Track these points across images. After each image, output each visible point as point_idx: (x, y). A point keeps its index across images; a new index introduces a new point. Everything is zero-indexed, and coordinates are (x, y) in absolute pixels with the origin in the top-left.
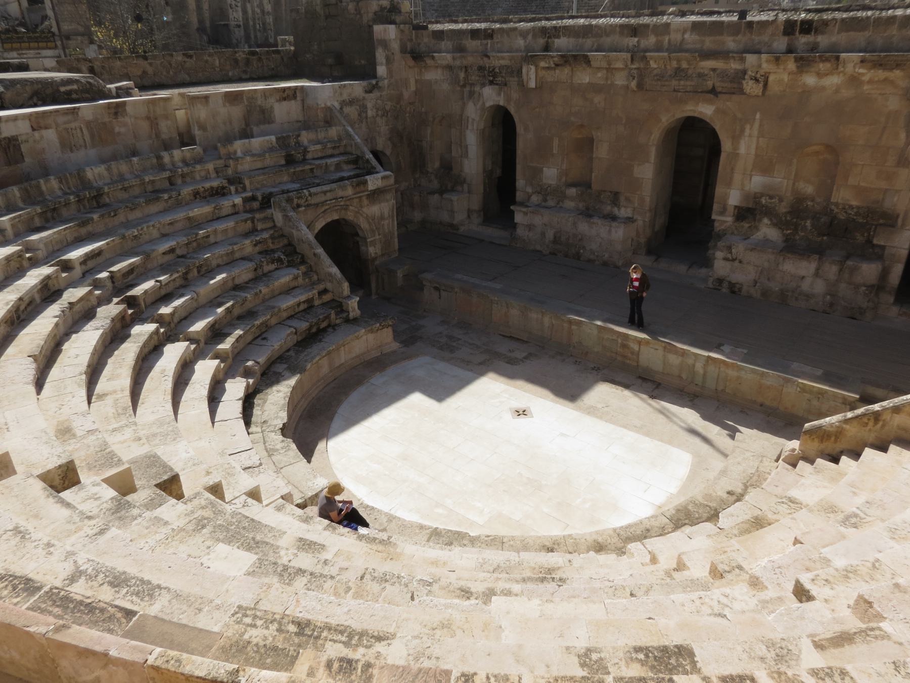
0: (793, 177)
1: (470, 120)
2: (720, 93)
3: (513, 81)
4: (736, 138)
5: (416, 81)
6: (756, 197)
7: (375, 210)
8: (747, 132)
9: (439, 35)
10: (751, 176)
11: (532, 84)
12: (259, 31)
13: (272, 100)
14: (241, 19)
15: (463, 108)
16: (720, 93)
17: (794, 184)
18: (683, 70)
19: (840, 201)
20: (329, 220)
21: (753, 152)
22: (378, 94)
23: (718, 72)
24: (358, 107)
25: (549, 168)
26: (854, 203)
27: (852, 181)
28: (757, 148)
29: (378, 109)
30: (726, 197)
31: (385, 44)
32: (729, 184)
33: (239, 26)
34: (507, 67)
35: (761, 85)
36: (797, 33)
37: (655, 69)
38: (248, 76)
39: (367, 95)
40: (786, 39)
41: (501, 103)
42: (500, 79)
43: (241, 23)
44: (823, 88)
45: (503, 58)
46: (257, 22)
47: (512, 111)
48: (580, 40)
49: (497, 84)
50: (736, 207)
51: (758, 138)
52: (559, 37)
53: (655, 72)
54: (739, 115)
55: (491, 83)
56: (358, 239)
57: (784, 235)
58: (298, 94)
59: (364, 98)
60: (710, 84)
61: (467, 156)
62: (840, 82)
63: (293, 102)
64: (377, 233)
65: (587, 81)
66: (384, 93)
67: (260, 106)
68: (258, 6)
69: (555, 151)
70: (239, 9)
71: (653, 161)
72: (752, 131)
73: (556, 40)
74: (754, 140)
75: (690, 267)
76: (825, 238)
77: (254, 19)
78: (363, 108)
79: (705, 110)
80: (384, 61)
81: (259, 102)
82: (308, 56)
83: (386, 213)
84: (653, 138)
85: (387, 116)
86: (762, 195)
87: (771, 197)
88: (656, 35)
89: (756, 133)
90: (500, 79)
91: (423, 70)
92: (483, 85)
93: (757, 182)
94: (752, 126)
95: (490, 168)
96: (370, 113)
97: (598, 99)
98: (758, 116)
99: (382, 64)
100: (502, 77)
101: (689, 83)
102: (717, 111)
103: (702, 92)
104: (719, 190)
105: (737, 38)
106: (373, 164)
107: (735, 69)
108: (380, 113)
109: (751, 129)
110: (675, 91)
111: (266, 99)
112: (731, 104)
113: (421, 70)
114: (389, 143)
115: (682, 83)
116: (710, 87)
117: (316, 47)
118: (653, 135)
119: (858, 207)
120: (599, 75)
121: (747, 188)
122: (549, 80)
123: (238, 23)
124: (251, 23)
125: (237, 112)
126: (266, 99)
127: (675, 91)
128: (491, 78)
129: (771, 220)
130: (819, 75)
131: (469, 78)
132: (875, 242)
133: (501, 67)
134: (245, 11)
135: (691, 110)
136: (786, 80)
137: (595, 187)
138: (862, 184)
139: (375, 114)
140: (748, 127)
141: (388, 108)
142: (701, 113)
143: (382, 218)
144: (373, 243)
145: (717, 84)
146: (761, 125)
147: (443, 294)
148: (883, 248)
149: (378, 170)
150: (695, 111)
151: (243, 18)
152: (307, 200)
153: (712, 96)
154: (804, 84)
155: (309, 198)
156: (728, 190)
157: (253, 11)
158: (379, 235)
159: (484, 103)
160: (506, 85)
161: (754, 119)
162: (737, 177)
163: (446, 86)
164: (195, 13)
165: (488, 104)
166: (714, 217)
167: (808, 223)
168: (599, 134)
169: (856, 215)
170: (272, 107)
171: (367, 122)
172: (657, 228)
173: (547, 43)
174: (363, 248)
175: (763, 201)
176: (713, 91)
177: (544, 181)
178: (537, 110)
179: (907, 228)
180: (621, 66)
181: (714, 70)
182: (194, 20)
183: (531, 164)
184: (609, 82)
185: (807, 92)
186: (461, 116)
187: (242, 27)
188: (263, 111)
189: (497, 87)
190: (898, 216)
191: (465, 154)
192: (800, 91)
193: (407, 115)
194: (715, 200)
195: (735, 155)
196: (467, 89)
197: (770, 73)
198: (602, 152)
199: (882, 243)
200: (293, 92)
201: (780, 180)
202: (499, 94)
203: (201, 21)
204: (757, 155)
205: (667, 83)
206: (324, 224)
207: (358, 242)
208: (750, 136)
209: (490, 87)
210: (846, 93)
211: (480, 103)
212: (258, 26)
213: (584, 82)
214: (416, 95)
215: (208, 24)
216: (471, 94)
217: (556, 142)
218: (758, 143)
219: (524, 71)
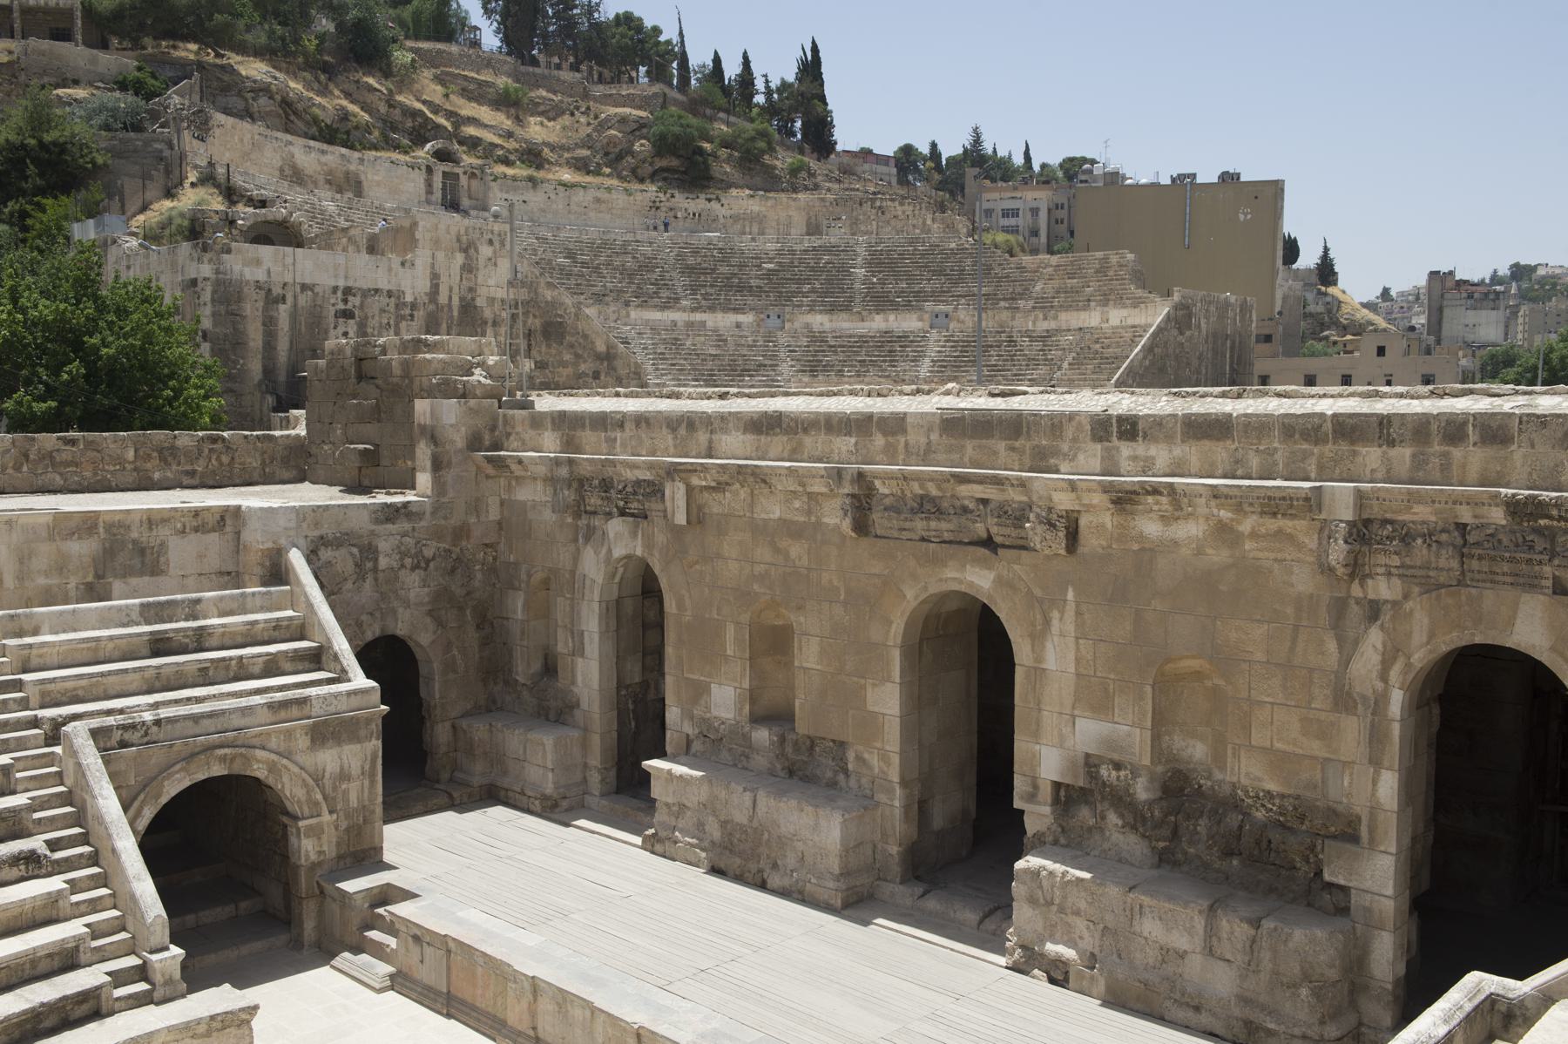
0: (1149, 724)
1: (588, 582)
2: (1004, 546)
3: (653, 506)
4: (1038, 636)
5: (502, 503)
6: (1090, 764)
7: (329, 759)
8: (1055, 623)
9: (538, 421)
10: (1074, 717)
11: (681, 519)
13: (164, 532)
15: (576, 558)
16: (1004, 546)
17: (1156, 738)
18: (932, 500)
19: (1244, 781)
20: (201, 777)
21: (1073, 670)
22: (407, 526)
23: (992, 506)
24: (355, 550)
25: (720, 684)
26: (1272, 786)
27: (1258, 738)
28: (1078, 661)
29: (403, 555)
30: (1034, 760)
31: (433, 438)
32: (1036, 735)
34: (649, 483)
35: (1062, 534)
36: (1115, 439)
37: (887, 496)
38: (196, 481)
39: (380, 528)
40: (1099, 446)
41: (639, 552)
42: (635, 505)
44: (1175, 543)
45: (634, 466)
47: (657, 571)
48: (763, 438)
49: (633, 515)
50: (1057, 786)
51: (1077, 638)
52: (725, 431)
53: (887, 501)
54: (1038, 592)
55: (623, 513)
56: (285, 819)
57: (1153, 848)
58: (229, 522)
59: (372, 533)
60: (980, 529)
61: (582, 655)
62: (1201, 534)
63: (214, 536)
64: (325, 808)
65: (777, 515)
66: (423, 523)
67: (134, 542)
69: (729, 652)
71: (898, 680)
72: (1063, 624)
73: (724, 437)
74: (1071, 641)
75: (986, 916)
76: (1235, 862)
78: (369, 551)
79: (979, 579)
80: (428, 464)
81: (135, 535)
82: (326, 447)
83: (355, 768)
84: (893, 630)
85: (426, 570)
86: (1102, 760)
87: (1118, 766)
88: (885, 434)
89: (1070, 628)
90: (635, 505)
91: (514, 483)
92: (609, 515)
93: (1089, 733)
94: (1062, 613)
95: (637, 679)
96: (383, 562)
97: (797, 550)
98: (1070, 595)
99: (424, 470)
100: (638, 501)
101: (944, 525)
102: (999, 581)
103: (970, 543)
104: (1021, 745)
105: (1017, 444)
106: (345, 663)
107: (1020, 502)
108: (408, 561)
109: (1061, 619)
110: (923, 539)
111: (150, 529)
112: (1018, 567)
113: (510, 484)
114: (428, 620)
115: (933, 524)
116: (985, 535)
117: (339, 432)
118: (894, 626)
119: (1283, 796)
120: (797, 504)
121: (1069, 743)
122: (715, 510)
125: (84, 549)
126: (150, 529)
127: (923, 539)
128: (621, 503)
129: (1121, 816)
130: (1165, 520)
131: (587, 501)
132: (1327, 877)
133: (638, 483)
135: (954, 579)
136: (1109, 525)
137: (802, 727)
138: (1278, 745)
139: (395, 565)
140: (1055, 614)
141: (428, 553)
142: (971, 584)
143: (344, 776)
144: (316, 832)
145: (994, 530)
146: (1078, 614)
147: (428, 950)
148: (1344, 890)
149: (351, 675)
150: (961, 582)
152: (146, 734)
153: (987, 552)
154: (1141, 536)
155: (155, 729)
156: (1038, 747)
158: (331, 812)
159: (610, 551)
160: (646, 517)
161: (1065, 601)
162: (1049, 719)
163: (548, 515)
164: (260, 356)
165: (618, 552)
166: (1017, 804)
167: (1203, 826)
168: (802, 619)
169: (1281, 814)
170: (162, 544)
171: (376, 580)
172: (938, 821)
173: (710, 441)
174: (293, 840)
175: (1105, 772)
176: (988, 543)
177: (715, 712)
178: (698, 567)
179: (1382, 848)
180: (824, 490)
181: (985, 502)
182: (255, 367)
183: (691, 676)
184: (813, 519)
185: (1149, 552)
186: (573, 573)
188: (141, 551)
189: (631, 519)
190: (1359, 819)
191: (579, 650)
192: (1136, 547)
193: (477, 567)
194: (1016, 767)
195: (1038, 673)
196: (583, 522)
197: (1079, 512)
198: (809, 656)
199: (1342, 882)
200: (217, 517)
201: (1126, 728)
202: (634, 535)
203: (269, 371)
204: (1078, 675)
205: (907, 525)
206: (187, 783)
207: (285, 826)
208: (1062, 635)
209: (620, 519)
210: (1218, 556)
211: (604, 551)
213: (772, 516)
214: (501, 529)
215: (282, 377)
216: (590, 533)
217: (730, 632)
218: (1078, 649)
219: (667, 492)
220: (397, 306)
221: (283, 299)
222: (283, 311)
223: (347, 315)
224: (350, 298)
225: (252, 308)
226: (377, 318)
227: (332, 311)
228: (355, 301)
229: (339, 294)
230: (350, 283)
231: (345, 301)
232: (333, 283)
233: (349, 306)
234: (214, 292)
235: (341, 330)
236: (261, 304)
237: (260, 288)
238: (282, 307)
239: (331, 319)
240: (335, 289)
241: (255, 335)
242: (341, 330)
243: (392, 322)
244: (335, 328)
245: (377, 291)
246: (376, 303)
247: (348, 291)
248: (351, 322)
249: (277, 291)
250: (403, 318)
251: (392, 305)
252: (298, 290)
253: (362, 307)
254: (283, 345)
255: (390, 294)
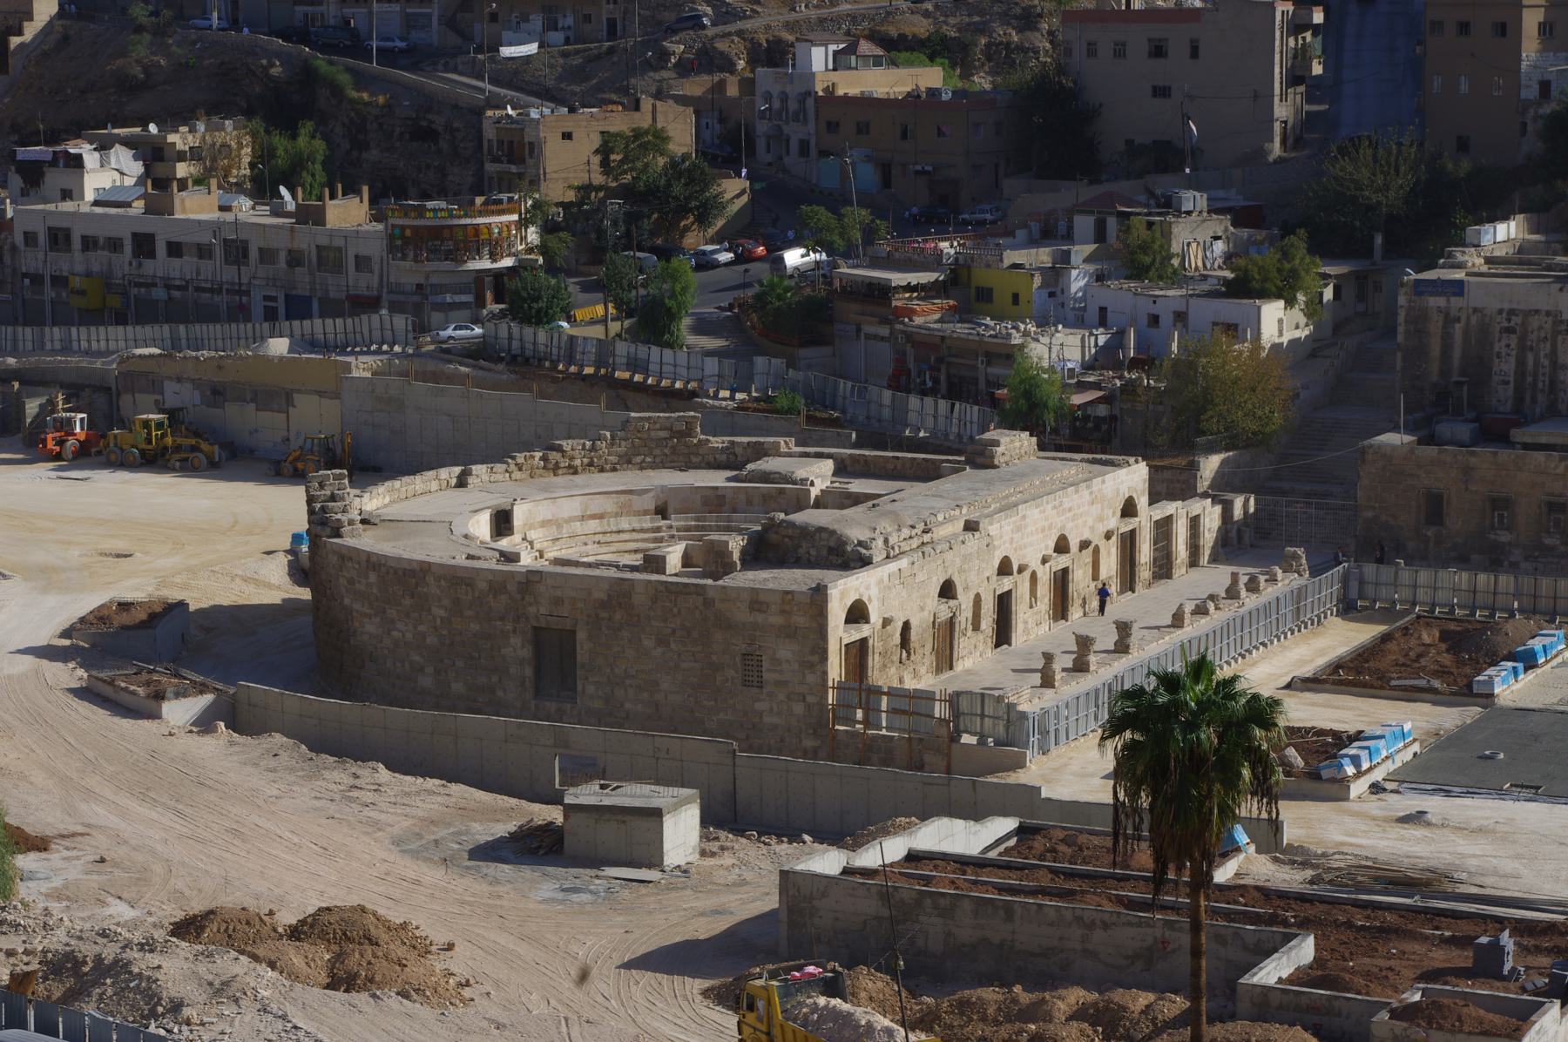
12: (1542, 391)
14: (1512, 373)
33: (1507, 383)
43: (1512, 379)
46: (1541, 378)
68: (1546, 355)
70: (1512, 360)
77: (1535, 375)
123: (1507, 379)
124: (1530, 379)
134: (1521, 362)
151: (1516, 373)
157: (1537, 364)
187: (1512, 385)
212: (1540, 385)
220: (1554, 323)
221: (1459, 320)
222: (1458, 328)
223: (1509, 331)
224: (1513, 318)
225: (1435, 325)
226: (1536, 333)
227: (1498, 328)
228: (1516, 320)
229: (1504, 315)
230: (1514, 306)
231: (1509, 320)
232: (1499, 306)
233: (1512, 323)
234: (1407, 315)
235: (1503, 343)
236: (1440, 324)
237: (1441, 312)
238: (1457, 326)
239: (1497, 335)
240: (1500, 312)
241: (1436, 349)
242: (1503, 343)
243: (1549, 336)
244: (1499, 341)
245: (1537, 311)
246: (1535, 322)
247: (1512, 312)
248: (1513, 336)
249: (1453, 313)
250: (1560, 332)
251: (1550, 322)
252: (1471, 311)
253: (1523, 323)
254: (1457, 354)
255: (1548, 313)
